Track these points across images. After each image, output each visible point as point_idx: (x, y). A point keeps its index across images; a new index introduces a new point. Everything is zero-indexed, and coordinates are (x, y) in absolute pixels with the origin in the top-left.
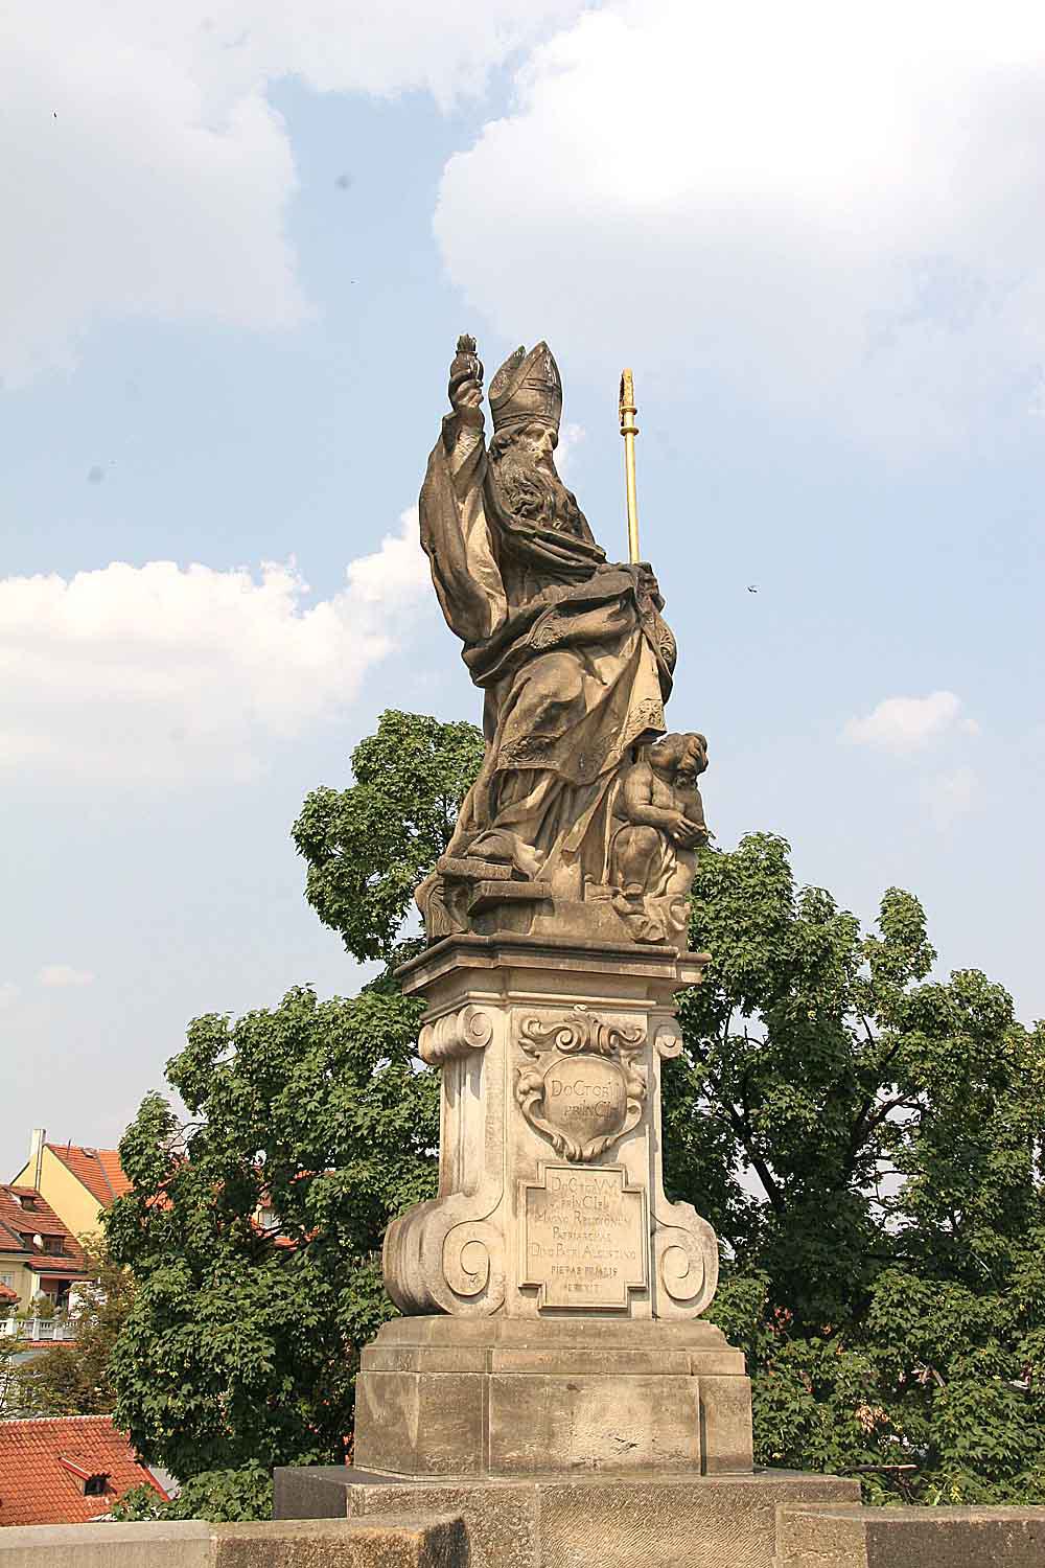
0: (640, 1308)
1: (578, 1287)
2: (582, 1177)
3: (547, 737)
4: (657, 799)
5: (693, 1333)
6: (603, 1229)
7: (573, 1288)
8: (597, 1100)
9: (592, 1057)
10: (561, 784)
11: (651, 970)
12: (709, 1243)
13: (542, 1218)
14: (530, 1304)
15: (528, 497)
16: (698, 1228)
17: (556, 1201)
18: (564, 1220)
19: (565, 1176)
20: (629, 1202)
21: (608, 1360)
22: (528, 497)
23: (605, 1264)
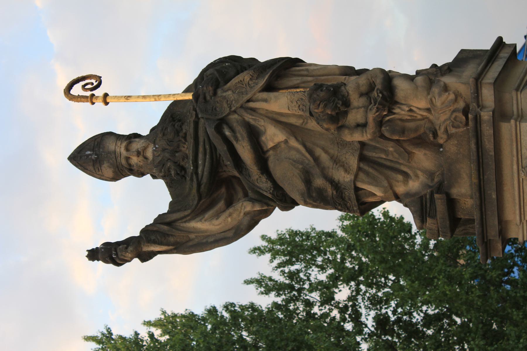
3: (333, 193)
4: (361, 120)
10: (362, 165)
15: (173, 172)
22: (173, 172)
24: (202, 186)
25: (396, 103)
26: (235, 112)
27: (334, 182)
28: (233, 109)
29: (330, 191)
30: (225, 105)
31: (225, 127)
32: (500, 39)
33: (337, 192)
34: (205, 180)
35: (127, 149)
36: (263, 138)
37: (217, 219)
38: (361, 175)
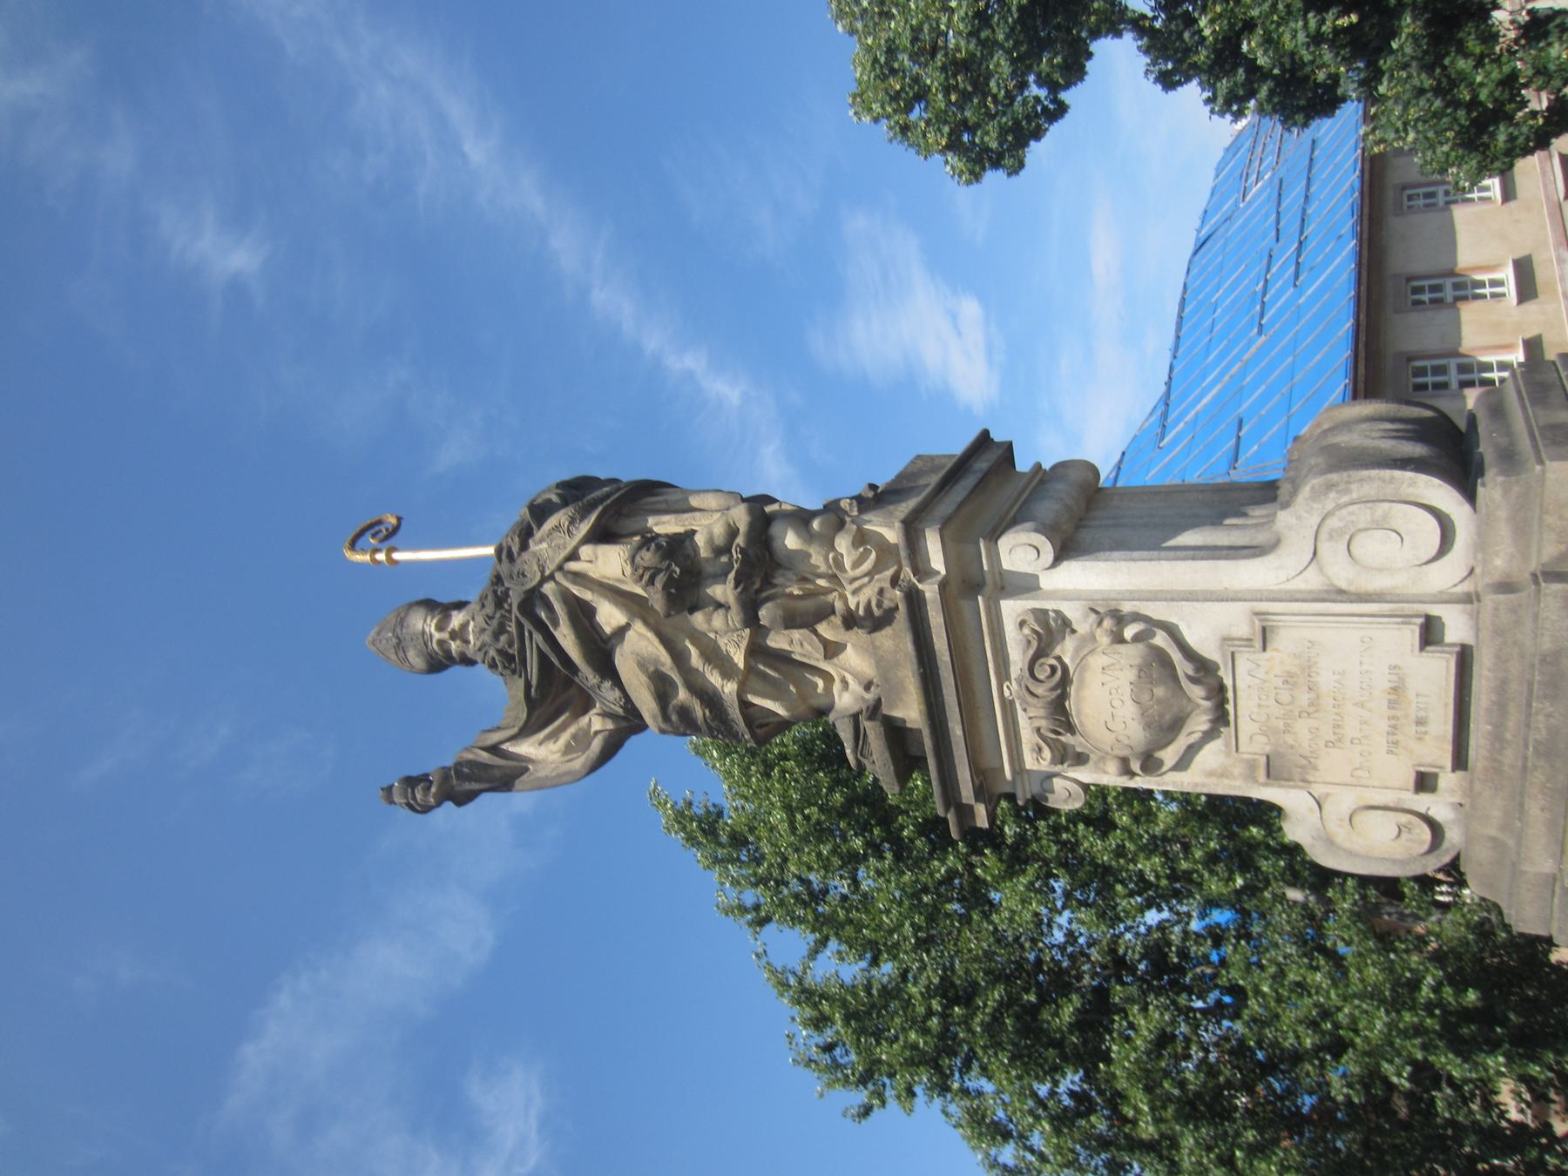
0: (1457, 628)
1: (1420, 722)
2: (1248, 705)
3: (704, 714)
5: (1504, 531)
6: (1325, 680)
7: (1422, 729)
8: (1129, 703)
9: (1071, 704)
11: (936, 619)
12: (1342, 486)
13: (1312, 760)
14: (1448, 780)
16: (1315, 505)
17: (1285, 742)
18: (1314, 731)
19: (1246, 727)
20: (1284, 642)
21: (1549, 716)
23: (1383, 682)
24: (533, 690)
25: (779, 566)
26: (552, 577)
27: (707, 693)
28: (547, 573)
29: (699, 711)
30: (536, 568)
31: (538, 603)
32: (985, 434)
33: (711, 712)
34: (534, 682)
35: (440, 628)
36: (598, 618)
37: (555, 743)
38: (754, 682)
